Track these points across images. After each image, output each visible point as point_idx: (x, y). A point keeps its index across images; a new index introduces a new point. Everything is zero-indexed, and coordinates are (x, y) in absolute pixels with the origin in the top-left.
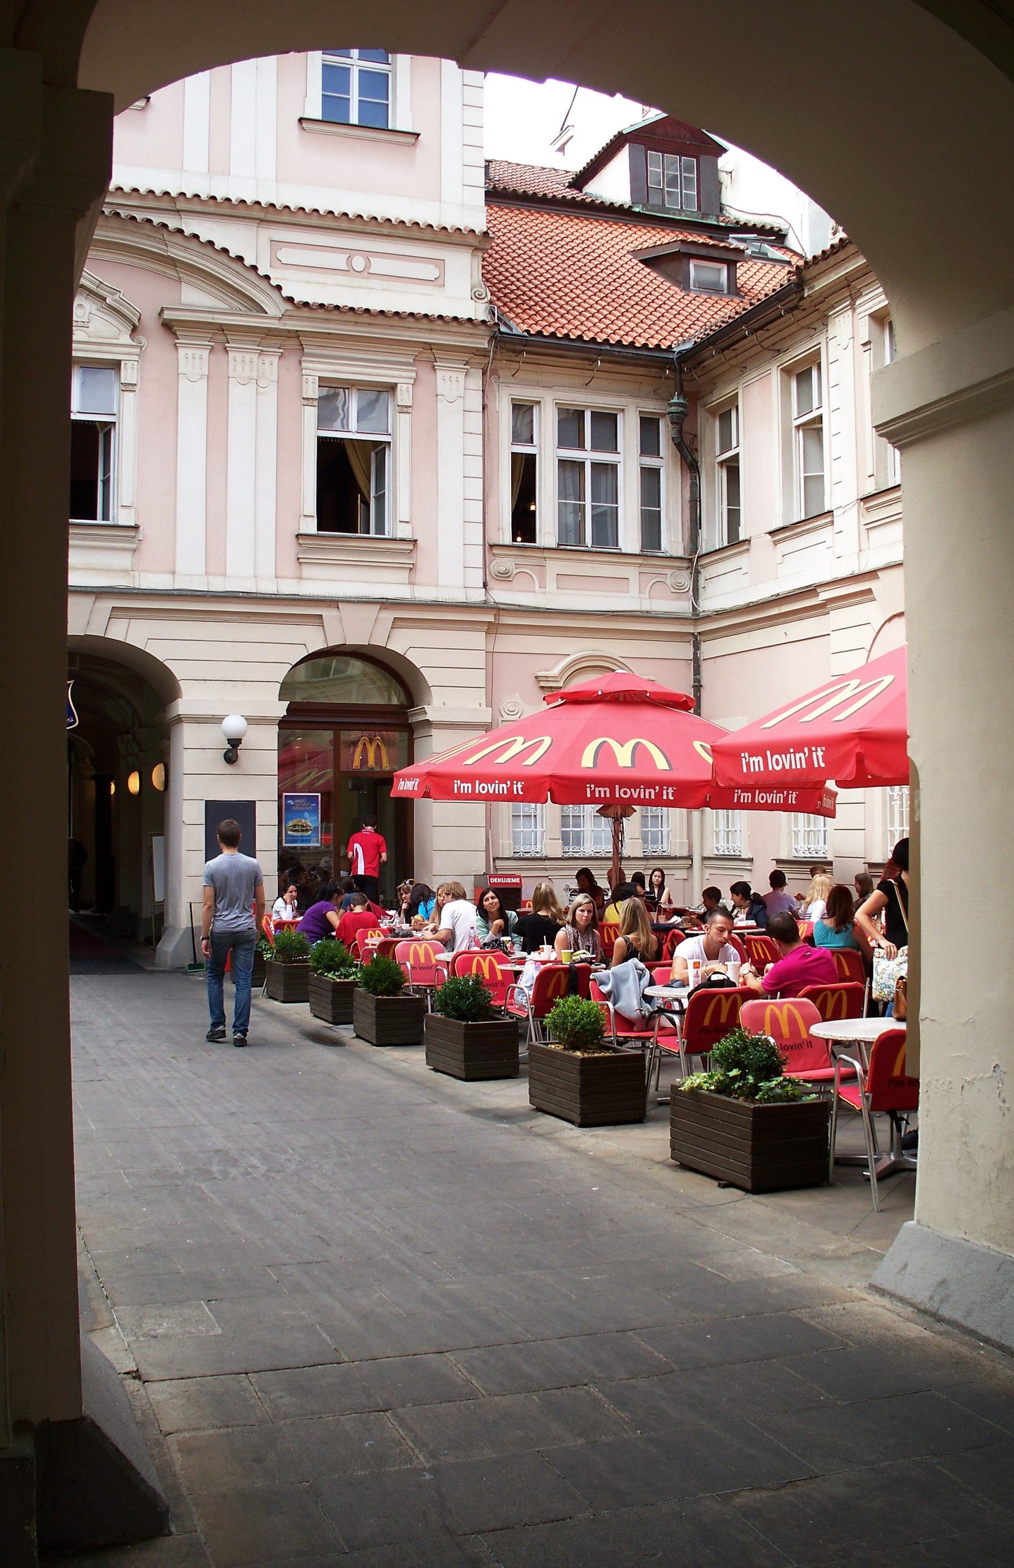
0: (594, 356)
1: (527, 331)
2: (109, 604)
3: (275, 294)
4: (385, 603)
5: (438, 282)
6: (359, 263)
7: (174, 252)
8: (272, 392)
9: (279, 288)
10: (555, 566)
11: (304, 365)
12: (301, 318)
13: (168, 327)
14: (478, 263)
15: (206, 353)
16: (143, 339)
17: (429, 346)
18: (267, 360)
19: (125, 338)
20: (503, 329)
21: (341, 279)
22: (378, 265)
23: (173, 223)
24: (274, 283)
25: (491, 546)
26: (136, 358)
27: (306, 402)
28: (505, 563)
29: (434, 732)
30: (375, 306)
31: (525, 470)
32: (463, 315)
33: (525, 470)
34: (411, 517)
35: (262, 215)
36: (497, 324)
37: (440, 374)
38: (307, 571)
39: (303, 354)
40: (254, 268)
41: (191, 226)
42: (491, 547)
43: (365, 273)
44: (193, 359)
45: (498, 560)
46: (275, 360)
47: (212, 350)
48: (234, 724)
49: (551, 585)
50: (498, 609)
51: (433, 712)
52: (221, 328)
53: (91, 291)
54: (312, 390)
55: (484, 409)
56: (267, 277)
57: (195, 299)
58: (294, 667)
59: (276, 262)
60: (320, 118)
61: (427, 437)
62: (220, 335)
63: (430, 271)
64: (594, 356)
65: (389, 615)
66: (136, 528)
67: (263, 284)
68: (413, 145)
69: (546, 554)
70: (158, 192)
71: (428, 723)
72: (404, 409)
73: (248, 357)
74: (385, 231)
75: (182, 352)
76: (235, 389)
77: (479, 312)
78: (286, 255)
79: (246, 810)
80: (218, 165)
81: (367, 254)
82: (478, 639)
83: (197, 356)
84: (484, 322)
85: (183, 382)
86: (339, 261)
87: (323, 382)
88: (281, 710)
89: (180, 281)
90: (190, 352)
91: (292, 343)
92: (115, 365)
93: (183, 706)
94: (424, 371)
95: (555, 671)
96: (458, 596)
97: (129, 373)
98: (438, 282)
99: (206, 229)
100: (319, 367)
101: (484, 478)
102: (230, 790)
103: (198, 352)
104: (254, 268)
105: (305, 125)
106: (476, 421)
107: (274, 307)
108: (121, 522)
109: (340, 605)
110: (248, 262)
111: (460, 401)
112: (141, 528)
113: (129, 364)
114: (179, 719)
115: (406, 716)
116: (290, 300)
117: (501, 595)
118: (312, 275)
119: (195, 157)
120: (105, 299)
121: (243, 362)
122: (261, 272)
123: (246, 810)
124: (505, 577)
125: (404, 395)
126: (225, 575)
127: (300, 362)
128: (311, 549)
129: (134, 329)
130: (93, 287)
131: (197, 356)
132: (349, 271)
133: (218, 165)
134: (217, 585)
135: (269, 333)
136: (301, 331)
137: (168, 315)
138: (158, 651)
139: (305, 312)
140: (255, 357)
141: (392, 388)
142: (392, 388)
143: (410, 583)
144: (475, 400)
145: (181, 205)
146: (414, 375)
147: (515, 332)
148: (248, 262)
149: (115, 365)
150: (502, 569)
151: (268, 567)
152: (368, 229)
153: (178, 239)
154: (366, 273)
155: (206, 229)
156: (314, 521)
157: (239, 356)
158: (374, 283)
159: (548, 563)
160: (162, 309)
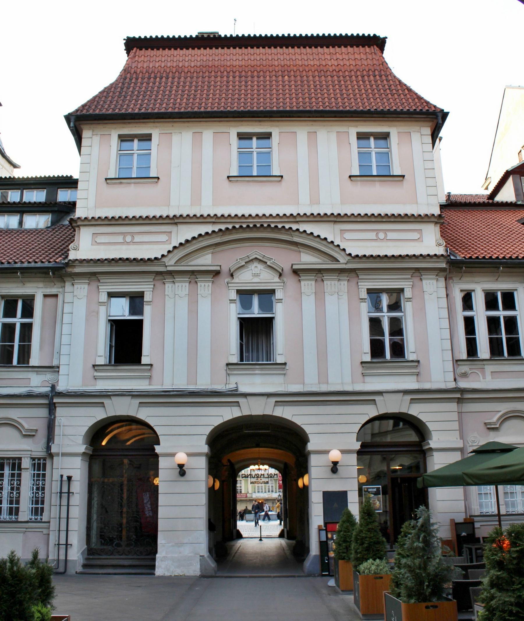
0: (498, 266)
1: (464, 257)
2: (273, 400)
3: (342, 253)
4: (406, 392)
5: (419, 240)
6: (381, 235)
7: (296, 239)
8: (345, 297)
9: (344, 250)
10: (490, 368)
11: (359, 284)
12: (355, 263)
13: (296, 272)
14: (438, 228)
15: (313, 283)
16: (285, 280)
17: (417, 270)
18: (342, 283)
19: (277, 279)
20: (452, 257)
21: (374, 244)
22: (391, 236)
23: (295, 227)
24: (342, 248)
25: (457, 361)
26: (282, 287)
27: (361, 301)
28: (464, 368)
29: (435, 453)
30: (389, 254)
31: (469, 323)
32: (432, 253)
33: (469, 323)
34: (416, 350)
35: (335, 219)
36: (449, 256)
37: (424, 282)
38: (367, 379)
39: (359, 279)
40: (332, 242)
41: (302, 227)
42: (457, 362)
43: (385, 239)
44: (308, 285)
45: (460, 367)
46: (346, 283)
47: (316, 280)
48: (335, 455)
49: (489, 377)
50: (463, 391)
51: (433, 443)
52: (320, 271)
53: (260, 260)
54: (364, 294)
55: (447, 296)
56: (338, 246)
57: (307, 259)
58: (364, 425)
59: (343, 239)
60: (358, 174)
61: (421, 311)
62: (319, 273)
63: (416, 236)
64: (498, 266)
65: (408, 397)
66: (285, 364)
67: (337, 249)
68: (402, 181)
69: (485, 363)
70: (288, 215)
71: (431, 449)
72: (409, 300)
73: (333, 282)
74: (392, 220)
75: (302, 283)
76: (328, 298)
77: (441, 251)
78: (347, 235)
79: (343, 495)
80: (315, 200)
81: (385, 231)
82: (454, 406)
83: (310, 284)
84: (442, 255)
85: (304, 297)
86: (372, 236)
87: (370, 291)
88: (357, 446)
89: (300, 252)
90: (306, 283)
91: (353, 275)
92: (273, 292)
93: (310, 447)
94: (416, 280)
95: (495, 419)
96: (443, 386)
97: (279, 295)
98: (419, 240)
99: (309, 228)
100: (367, 283)
101: (450, 329)
102: (335, 486)
103: (310, 282)
104: (332, 242)
105: (352, 178)
106: (444, 302)
107: (342, 259)
108: (278, 362)
109: (384, 394)
110: (329, 240)
111: (435, 294)
112: (288, 364)
113: (279, 290)
114: (309, 453)
115: (421, 446)
116: (350, 255)
117: (463, 384)
118: (359, 243)
119: (304, 196)
120: (266, 263)
121: (331, 285)
122: (336, 244)
123: (343, 495)
124: (465, 375)
125: (408, 293)
126: (328, 383)
127: (358, 283)
128: (368, 368)
129: (280, 275)
130: (261, 258)
131: (310, 284)
132: (377, 239)
133: (315, 200)
134: (324, 388)
135: (342, 271)
136: (355, 268)
137: (295, 267)
138: (298, 421)
139: (357, 260)
140: (336, 282)
141: (402, 290)
142: (402, 290)
143: (418, 381)
144: (443, 292)
145: (297, 220)
146: (412, 283)
147: (458, 258)
148: (329, 240)
149: (272, 292)
150: (463, 371)
151: (348, 379)
152: (384, 220)
153: (297, 233)
154: (385, 239)
155: (309, 228)
156: (369, 355)
157: (329, 282)
158: (390, 244)
159: (486, 367)
160: (292, 265)
